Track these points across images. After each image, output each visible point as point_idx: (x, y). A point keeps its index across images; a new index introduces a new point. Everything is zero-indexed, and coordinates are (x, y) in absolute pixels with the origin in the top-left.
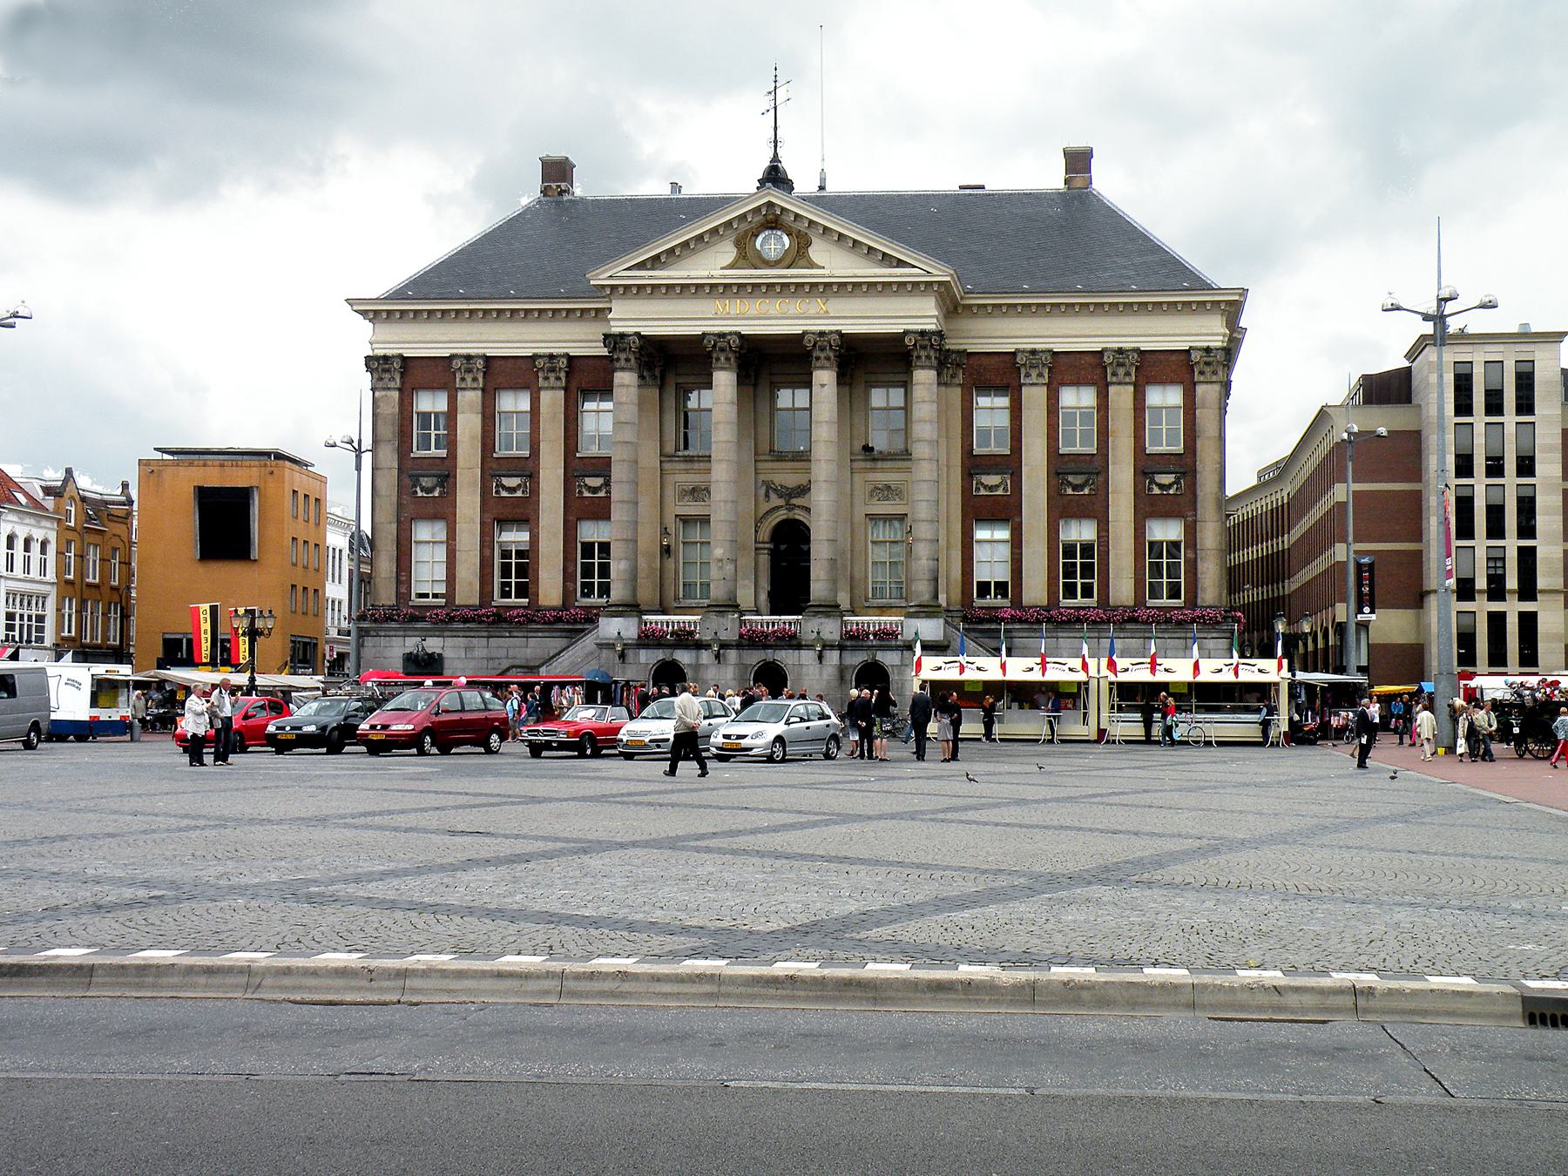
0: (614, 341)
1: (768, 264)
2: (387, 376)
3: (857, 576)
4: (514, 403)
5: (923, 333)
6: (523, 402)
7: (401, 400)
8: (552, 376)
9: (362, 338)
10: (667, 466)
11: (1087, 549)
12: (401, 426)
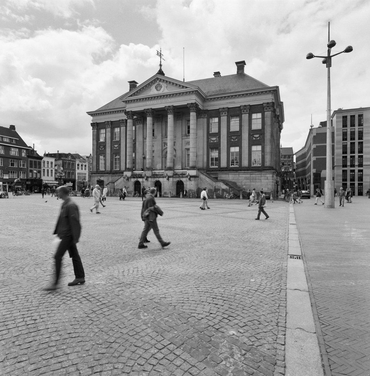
3: (184, 161)
5: (192, 104)
9: (90, 119)
12: (97, 136)
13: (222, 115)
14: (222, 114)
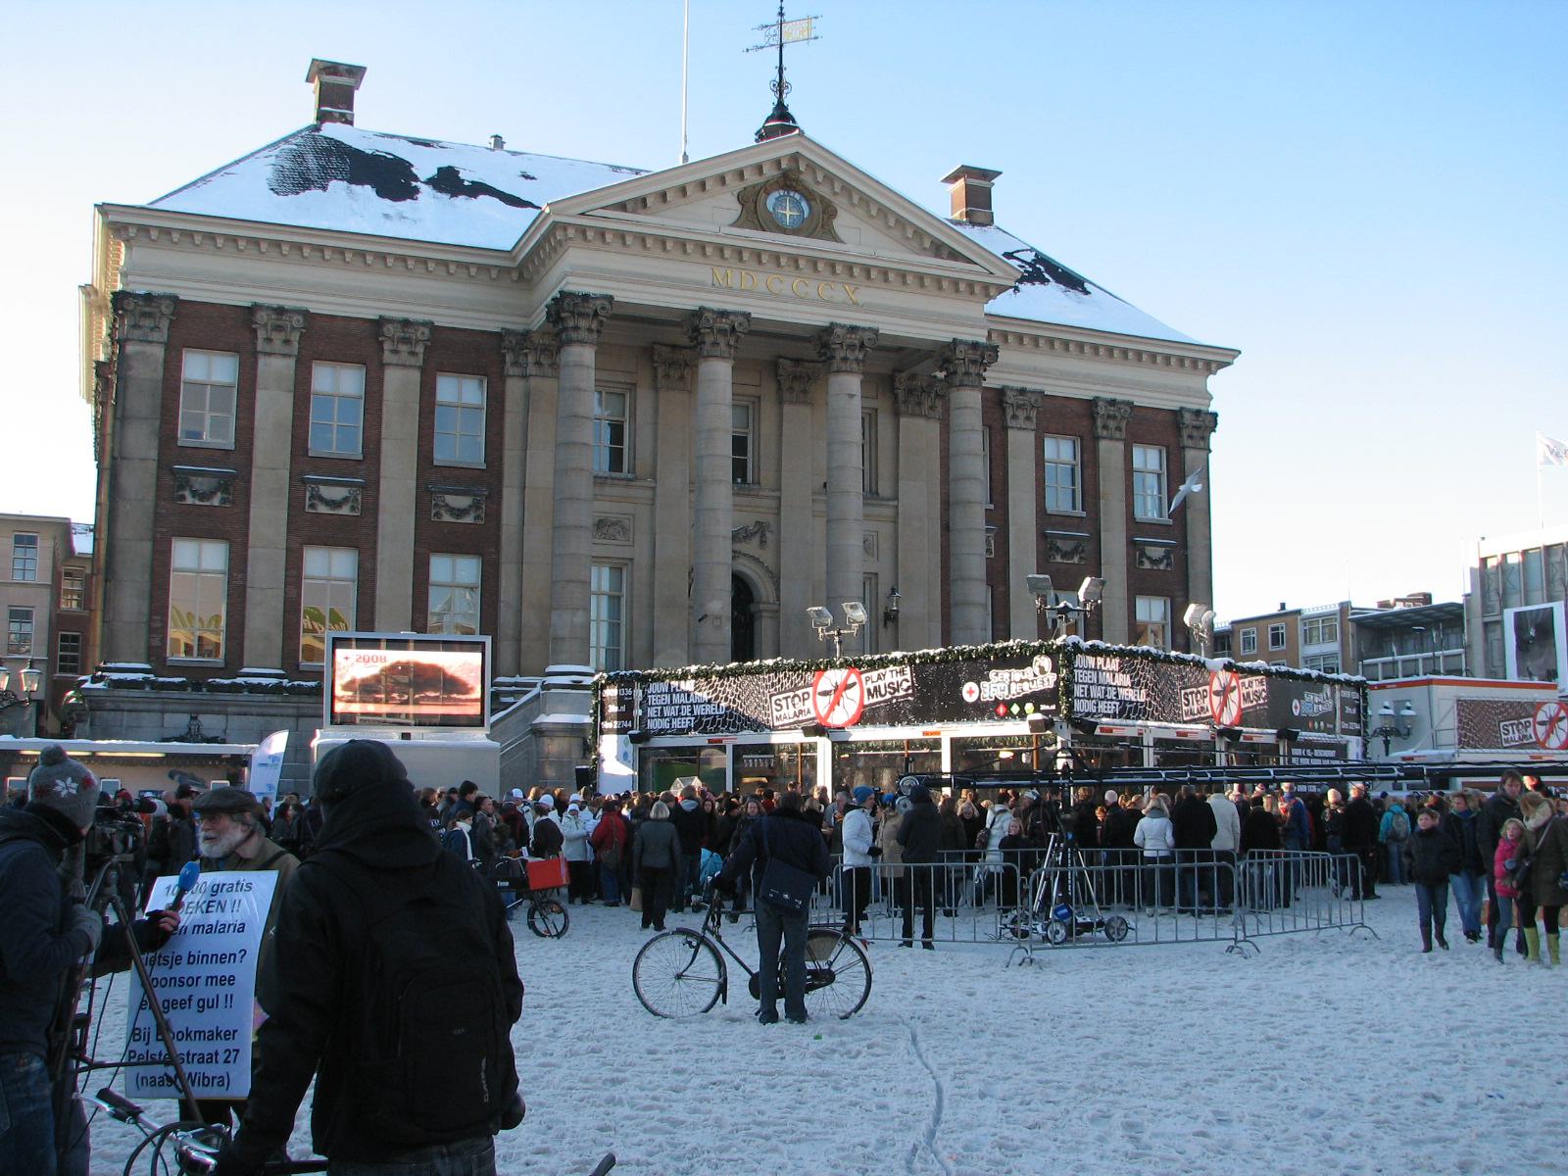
1: (783, 231)
2: (148, 323)
8: (403, 348)
14: (1014, 417)
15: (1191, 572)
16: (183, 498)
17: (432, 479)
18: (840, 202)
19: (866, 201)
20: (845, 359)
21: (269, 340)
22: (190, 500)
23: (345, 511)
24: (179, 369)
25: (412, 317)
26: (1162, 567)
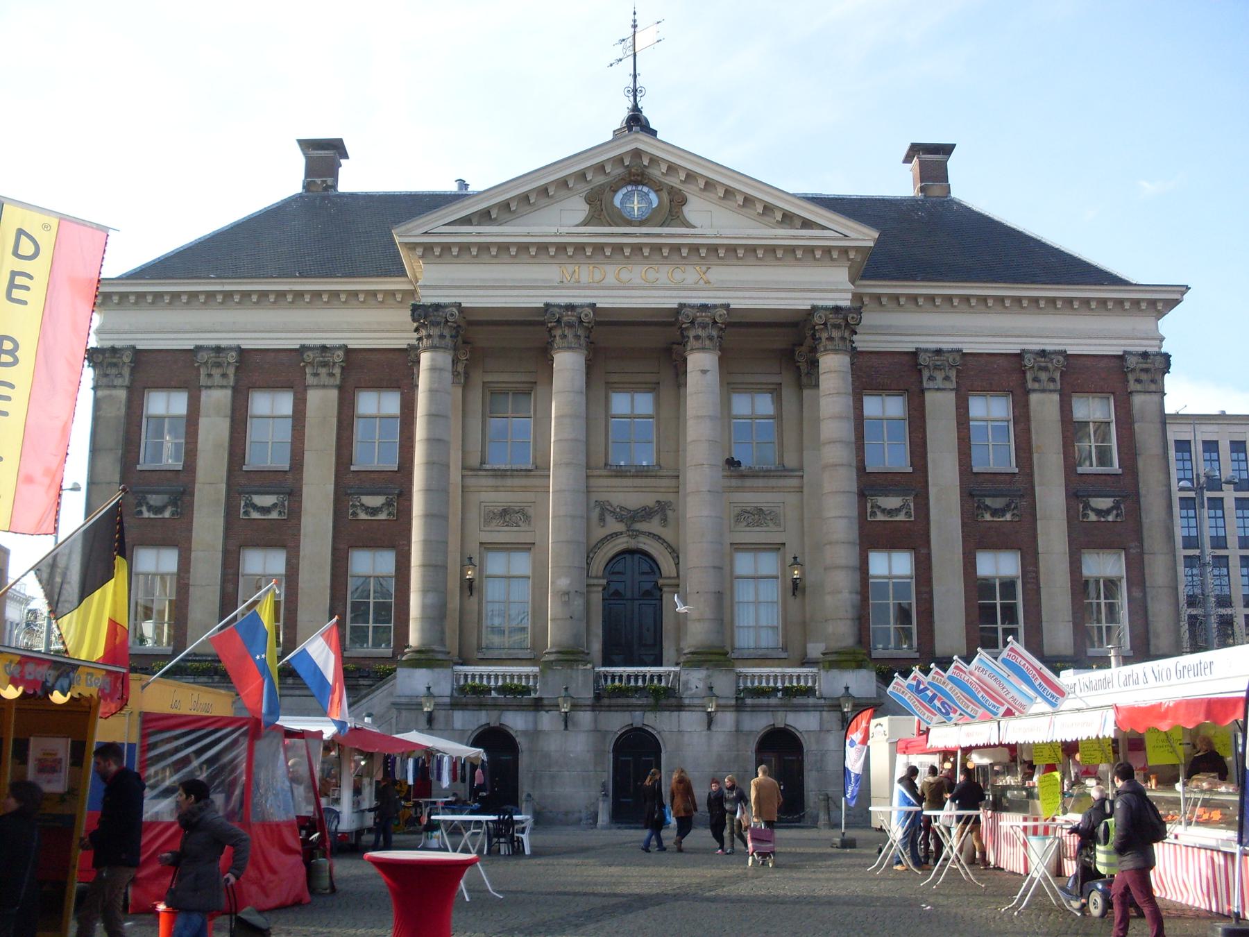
0: (424, 315)
1: (630, 223)
2: (113, 371)
4: (271, 406)
6: (284, 403)
7: (130, 401)
8: (323, 371)
10: (471, 482)
11: (1008, 586)
13: (931, 385)
14: (931, 378)
15: (1146, 521)
16: (141, 512)
17: (348, 483)
18: (688, 190)
19: (710, 185)
20: (697, 338)
21: (210, 375)
22: (146, 514)
23: (274, 515)
24: (189, 405)
25: (328, 343)
26: (1110, 518)
